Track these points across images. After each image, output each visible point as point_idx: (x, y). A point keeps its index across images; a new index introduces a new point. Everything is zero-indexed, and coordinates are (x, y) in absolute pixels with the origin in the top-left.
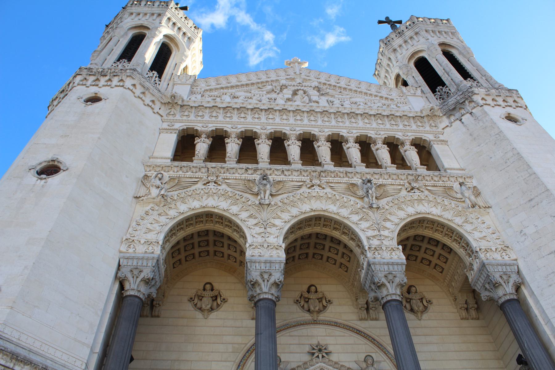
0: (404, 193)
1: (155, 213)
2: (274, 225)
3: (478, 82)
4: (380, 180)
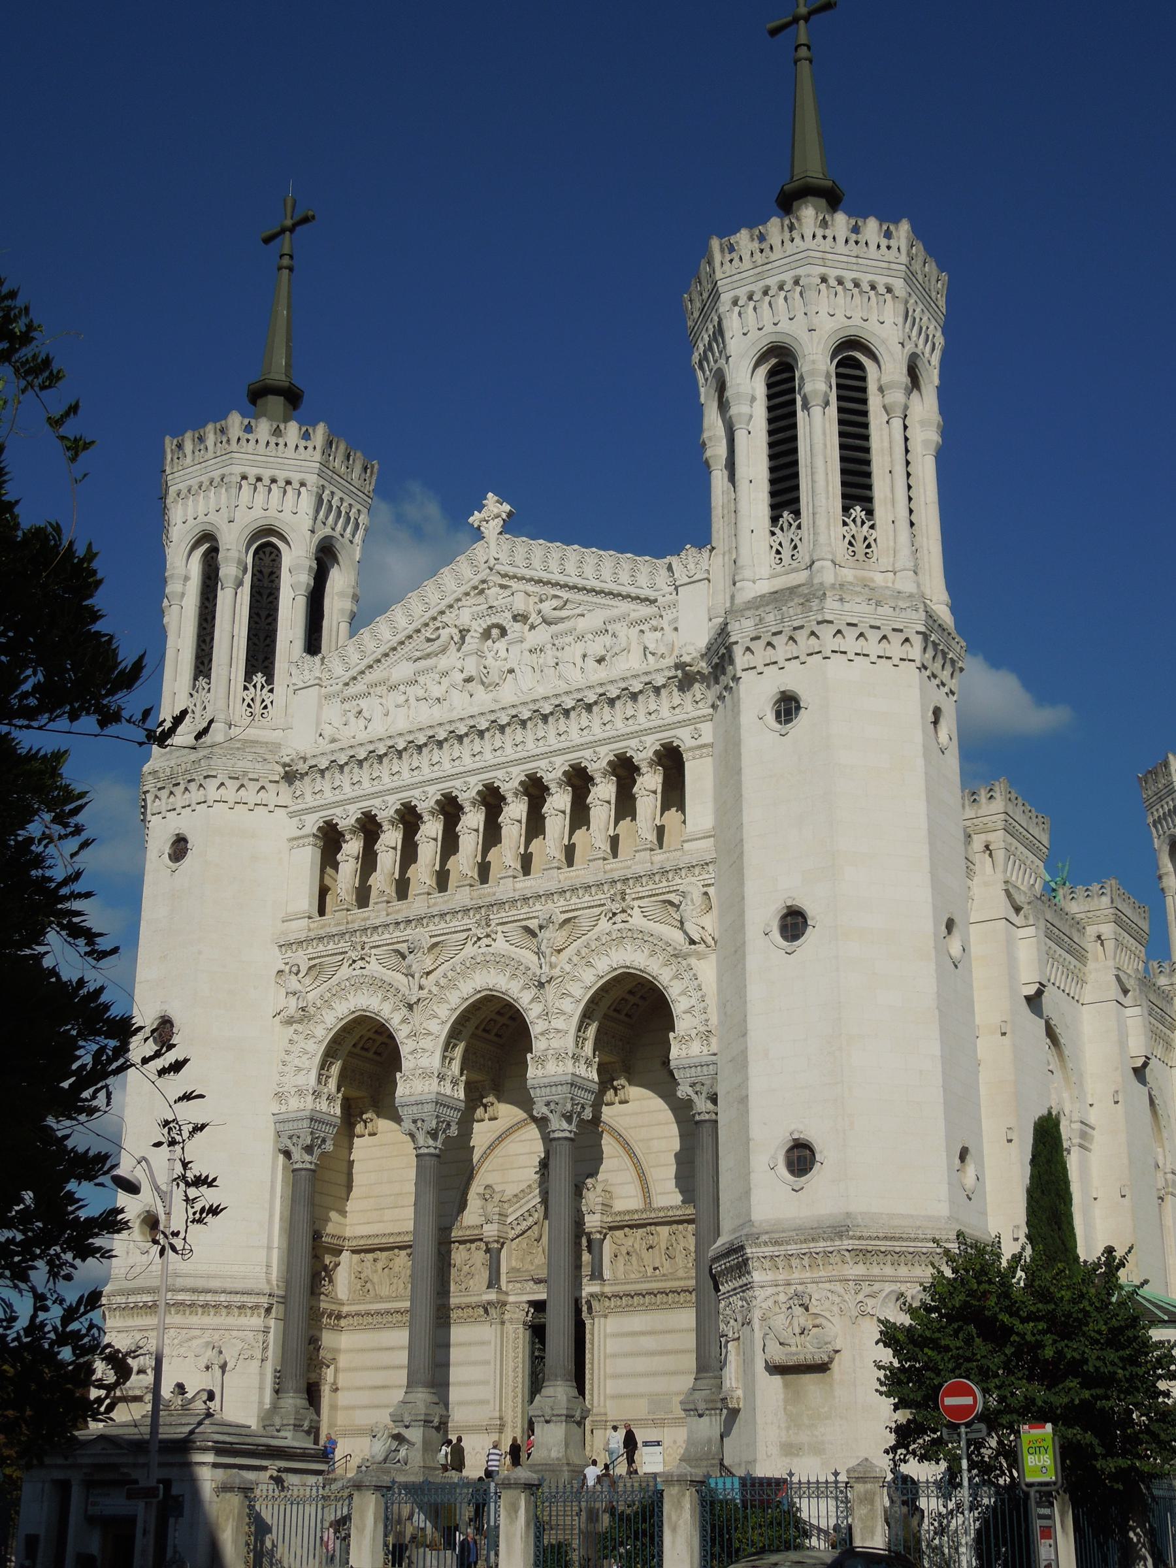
0: (604, 925)
1: (302, 1036)
2: (429, 1034)
3: (799, 527)
4: (572, 902)
